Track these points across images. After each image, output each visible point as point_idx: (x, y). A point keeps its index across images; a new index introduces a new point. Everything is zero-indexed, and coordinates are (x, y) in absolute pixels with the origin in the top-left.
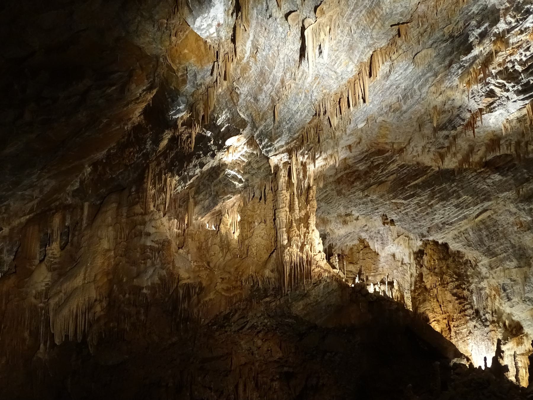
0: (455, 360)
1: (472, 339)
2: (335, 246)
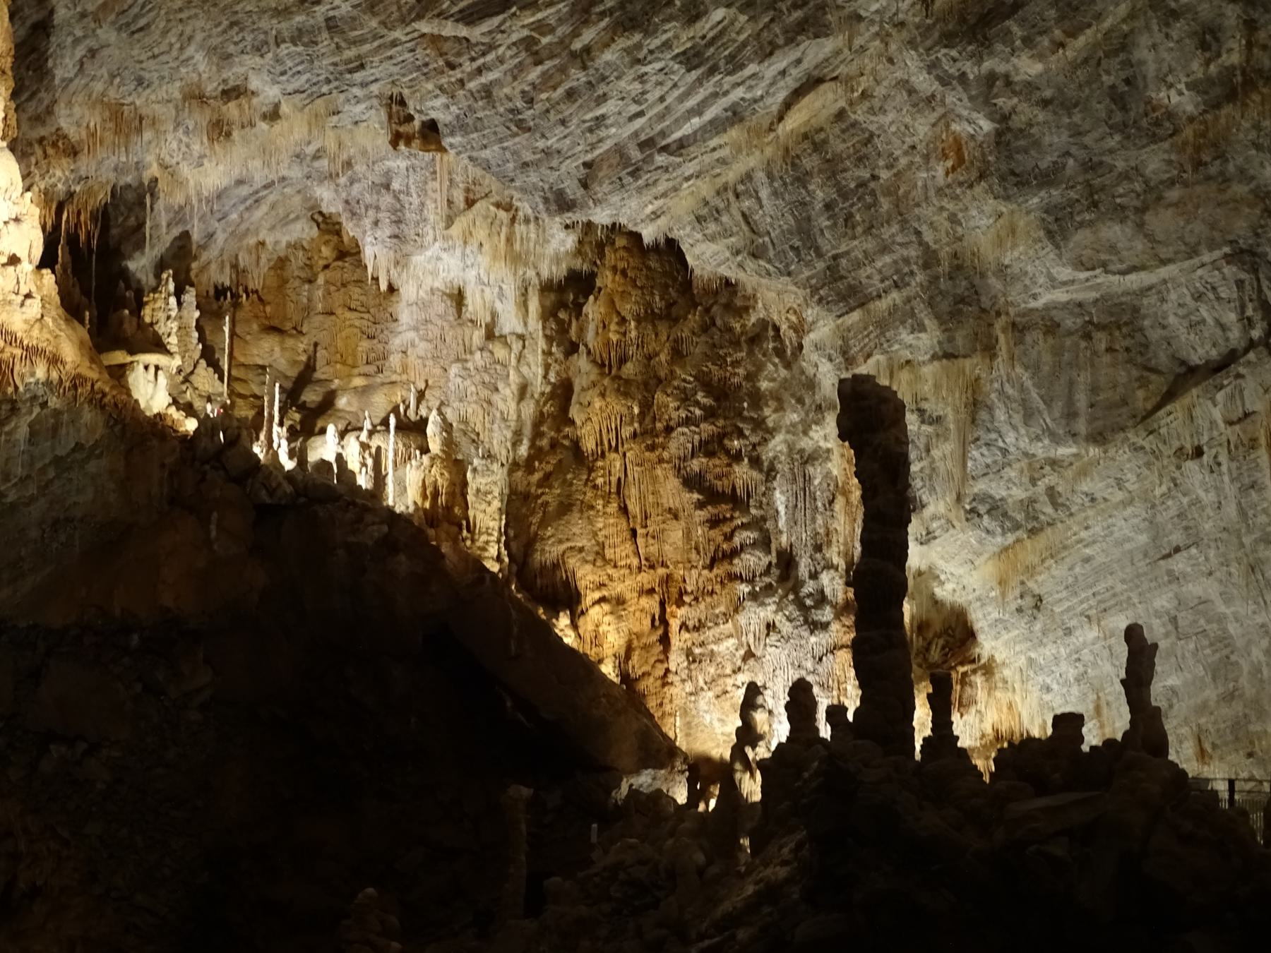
0: (645, 780)
2: (203, 247)
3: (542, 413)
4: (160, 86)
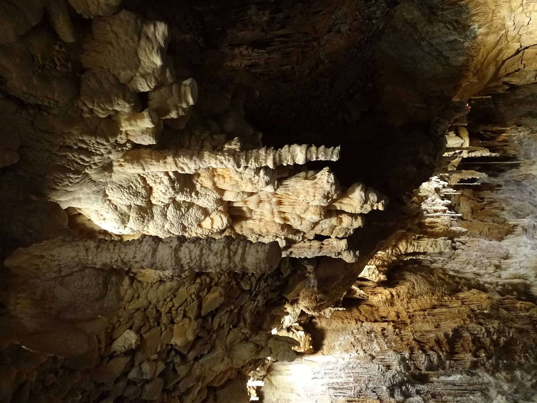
1: (358, 358)
3: (470, 280)
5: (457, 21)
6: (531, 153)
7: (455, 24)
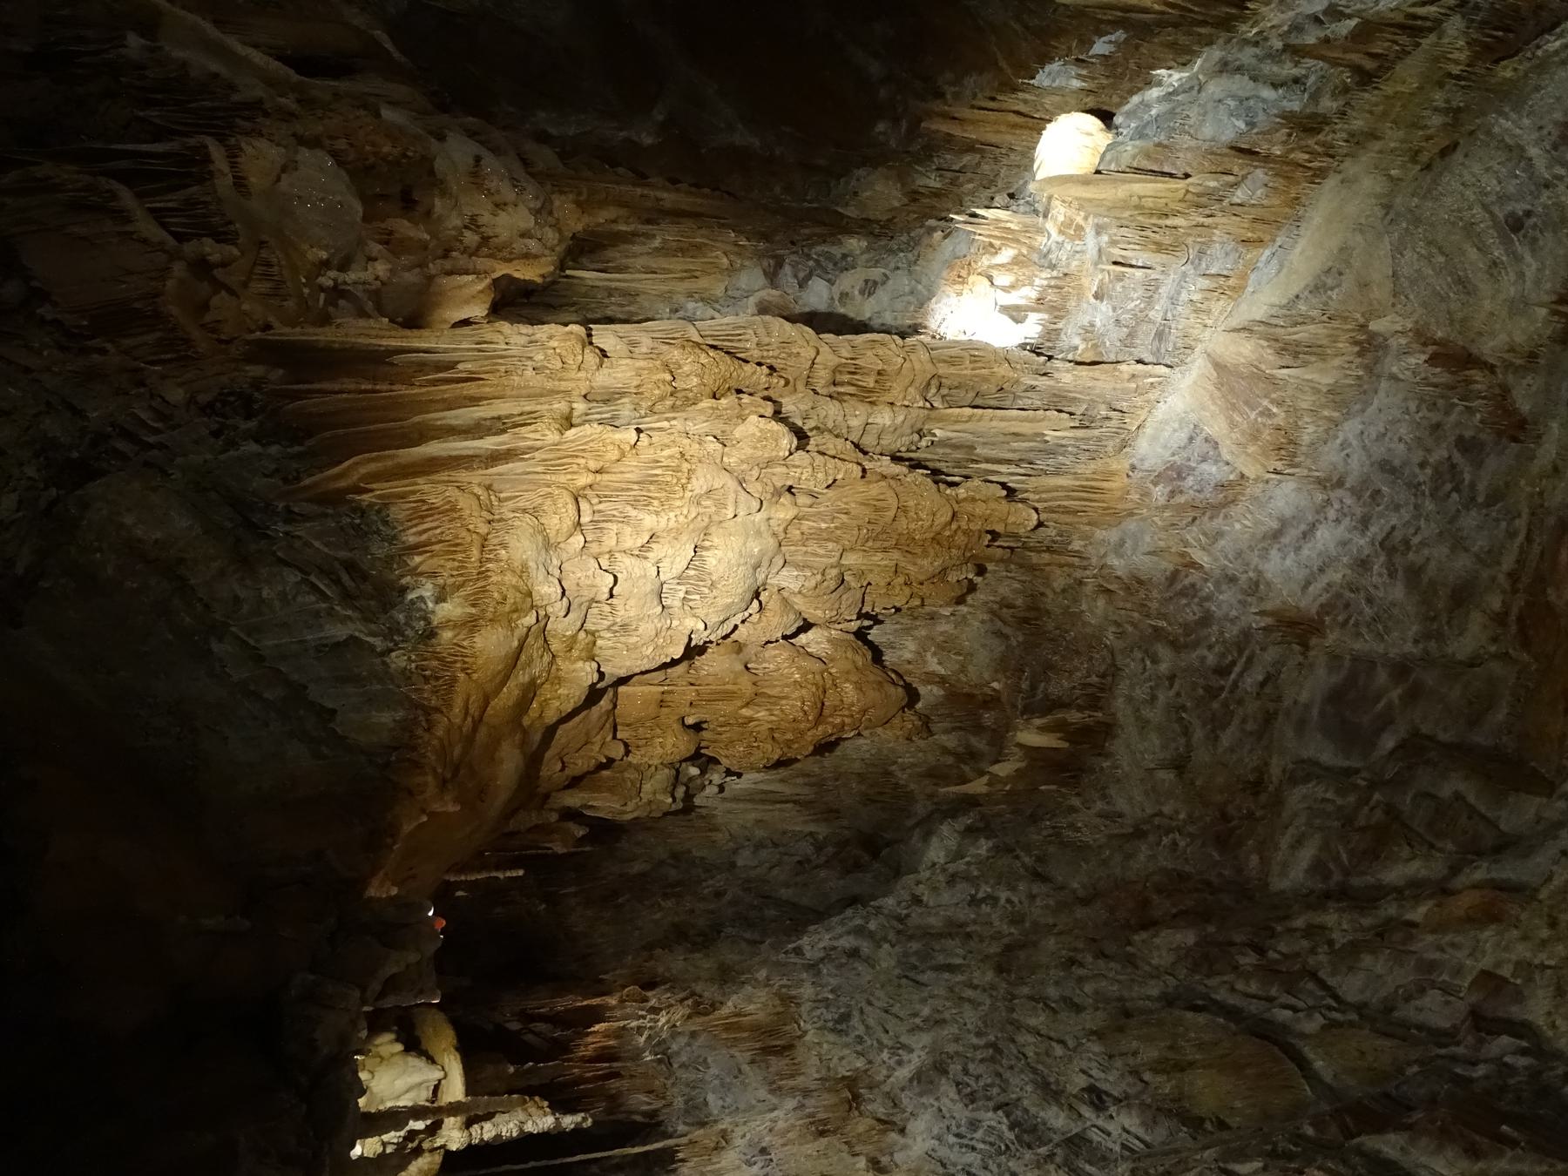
4: (846, 1045)
5: (350, 566)
6: (711, 1098)
7: (345, 578)
